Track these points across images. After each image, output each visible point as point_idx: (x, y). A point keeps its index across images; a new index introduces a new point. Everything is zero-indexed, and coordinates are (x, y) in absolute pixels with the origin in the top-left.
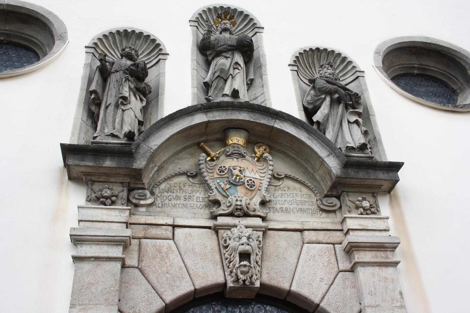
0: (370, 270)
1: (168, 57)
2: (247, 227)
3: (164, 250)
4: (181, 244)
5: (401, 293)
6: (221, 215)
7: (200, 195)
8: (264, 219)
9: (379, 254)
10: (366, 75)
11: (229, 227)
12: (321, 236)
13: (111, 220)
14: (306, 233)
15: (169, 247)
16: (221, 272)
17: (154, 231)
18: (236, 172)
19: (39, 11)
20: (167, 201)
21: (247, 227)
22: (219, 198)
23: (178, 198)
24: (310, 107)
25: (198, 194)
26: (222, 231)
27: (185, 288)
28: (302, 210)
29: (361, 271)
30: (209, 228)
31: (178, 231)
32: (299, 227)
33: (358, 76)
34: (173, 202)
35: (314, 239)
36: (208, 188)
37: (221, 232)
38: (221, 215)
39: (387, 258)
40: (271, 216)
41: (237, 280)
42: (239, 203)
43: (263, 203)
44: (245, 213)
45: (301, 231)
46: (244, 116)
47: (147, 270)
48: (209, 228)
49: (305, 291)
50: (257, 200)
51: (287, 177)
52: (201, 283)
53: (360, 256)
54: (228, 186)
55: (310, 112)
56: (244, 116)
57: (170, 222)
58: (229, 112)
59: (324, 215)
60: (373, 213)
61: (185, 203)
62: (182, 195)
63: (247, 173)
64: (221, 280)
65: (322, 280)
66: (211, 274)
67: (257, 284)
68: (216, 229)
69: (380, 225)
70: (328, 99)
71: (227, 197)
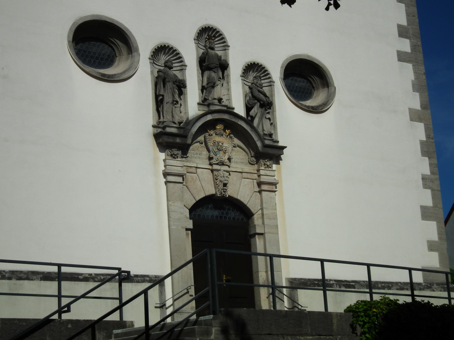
0: (266, 193)
1: (187, 67)
2: (224, 171)
3: (194, 178)
4: (200, 176)
5: (276, 204)
6: (214, 164)
7: (205, 152)
8: (229, 167)
9: (271, 186)
10: (275, 84)
11: (218, 170)
12: (249, 176)
13: (177, 165)
14: (244, 174)
15: (196, 177)
16: (214, 189)
17: (190, 170)
18: (220, 144)
19: (132, 39)
20: (193, 155)
21: (224, 171)
22: (213, 156)
23: (197, 154)
24: (249, 106)
25: (204, 153)
26: (215, 172)
27: (202, 195)
28: (242, 163)
29: (263, 192)
30: (209, 169)
31: (198, 170)
32: (241, 171)
33: (271, 84)
34: (195, 156)
35: (246, 177)
36: (208, 150)
37: (215, 172)
38: (214, 164)
39: (273, 188)
40: (231, 166)
41: (221, 193)
42: (221, 160)
43: (229, 159)
44: (222, 164)
45: (241, 172)
46: (226, 117)
47: (189, 187)
48: (209, 169)
49: (242, 200)
50: (227, 157)
51: (238, 146)
52: (208, 193)
53: (264, 187)
54: (217, 150)
55: (248, 109)
56: (226, 117)
57: (196, 166)
58: (221, 114)
59: (250, 165)
60: (270, 168)
61: (200, 156)
62: (198, 152)
63: (224, 145)
64: (214, 193)
65: (248, 195)
66: (210, 190)
67: (227, 196)
68: (212, 171)
69: (272, 173)
70: (258, 104)
71: (216, 155)
